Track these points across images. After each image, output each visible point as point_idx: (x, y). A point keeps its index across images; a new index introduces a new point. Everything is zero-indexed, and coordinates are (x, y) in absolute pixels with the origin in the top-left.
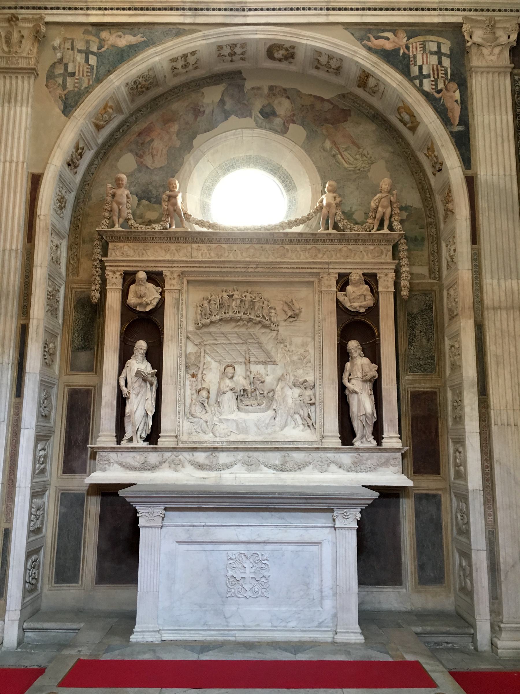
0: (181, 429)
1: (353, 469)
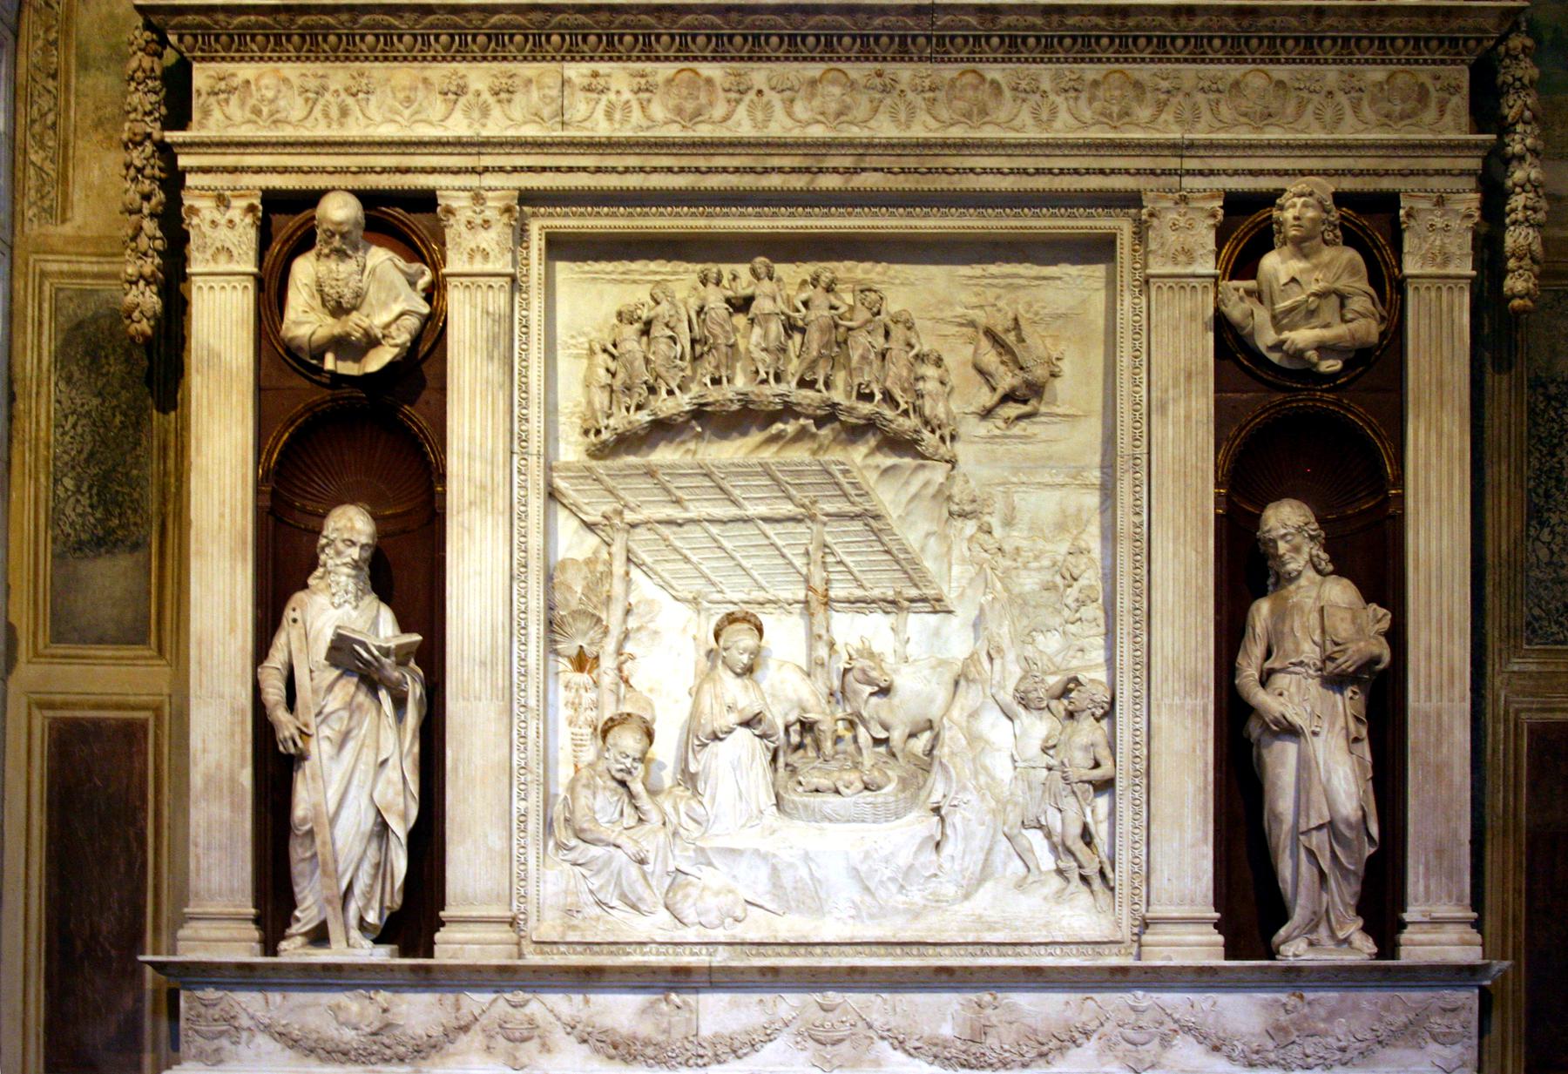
0: (532, 890)
1: (1272, 1056)
